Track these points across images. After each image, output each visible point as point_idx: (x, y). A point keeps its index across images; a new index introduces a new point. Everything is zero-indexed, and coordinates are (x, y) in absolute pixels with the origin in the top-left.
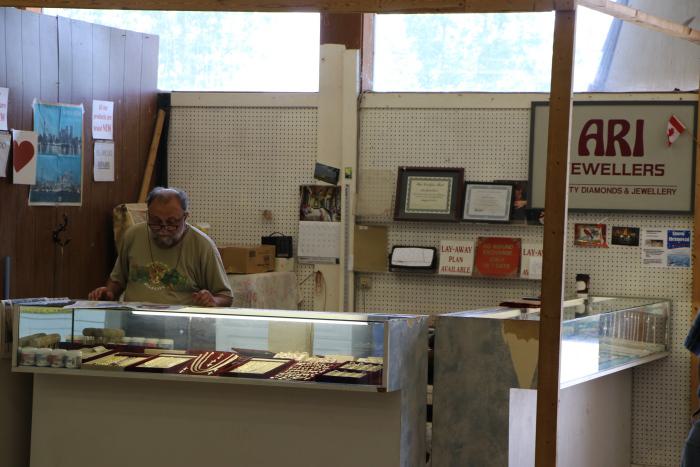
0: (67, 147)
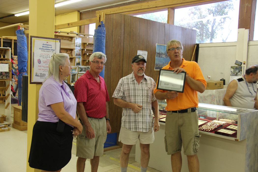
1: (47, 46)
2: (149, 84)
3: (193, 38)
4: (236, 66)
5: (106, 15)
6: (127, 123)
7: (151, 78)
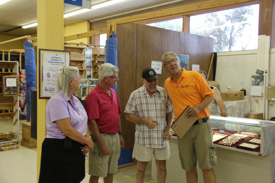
0: (183, 66)
3: (210, 47)
4: (258, 76)
5: (117, 24)
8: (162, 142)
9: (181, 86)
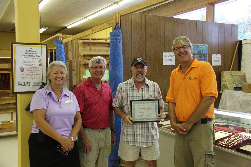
0: (201, 56)
1: (31, 53)
2: (151, 90)
5: (121, 16)
6: (125, 136)
7: (155, 83)
8: (146, 140)
9: (189, 78)
